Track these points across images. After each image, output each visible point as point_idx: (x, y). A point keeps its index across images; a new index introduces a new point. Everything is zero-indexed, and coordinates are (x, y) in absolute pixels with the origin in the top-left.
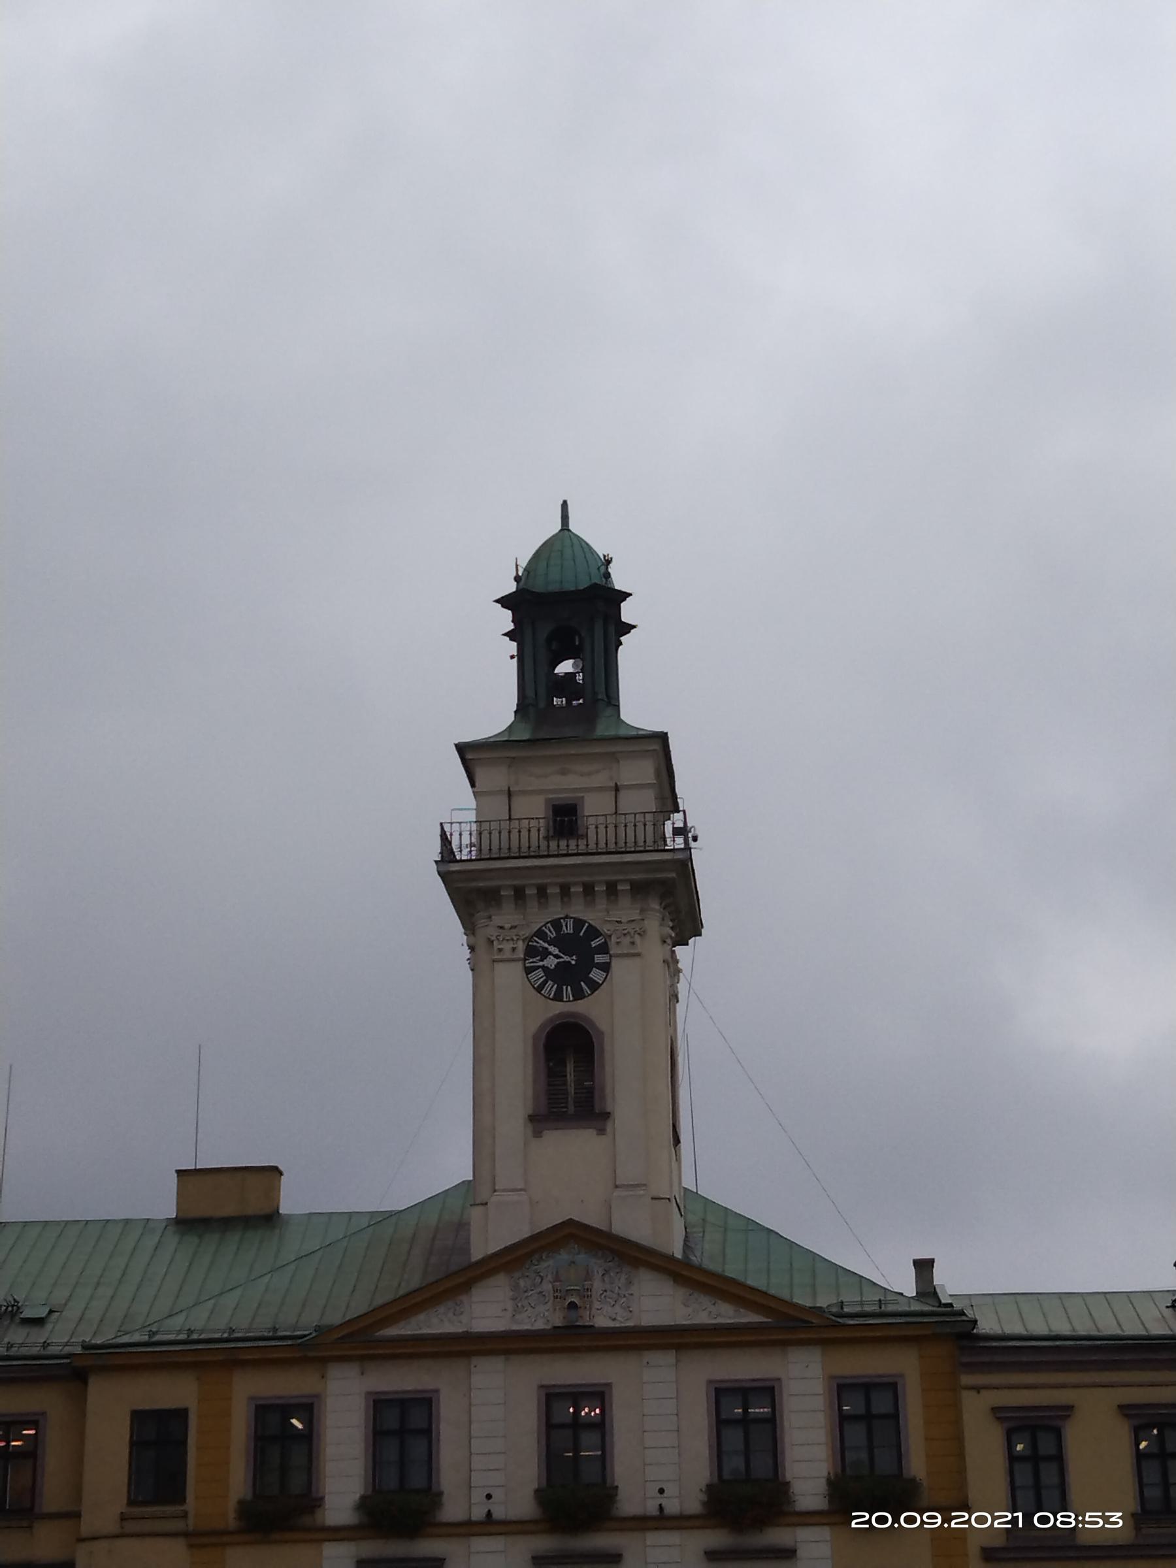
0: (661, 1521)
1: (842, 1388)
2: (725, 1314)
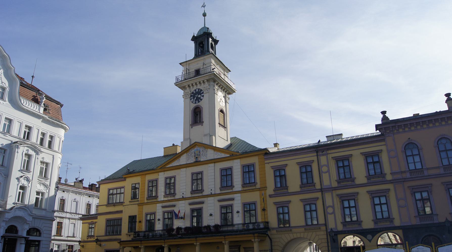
0: (211, 195)
1: (243, 167)
2: (223, 155)
